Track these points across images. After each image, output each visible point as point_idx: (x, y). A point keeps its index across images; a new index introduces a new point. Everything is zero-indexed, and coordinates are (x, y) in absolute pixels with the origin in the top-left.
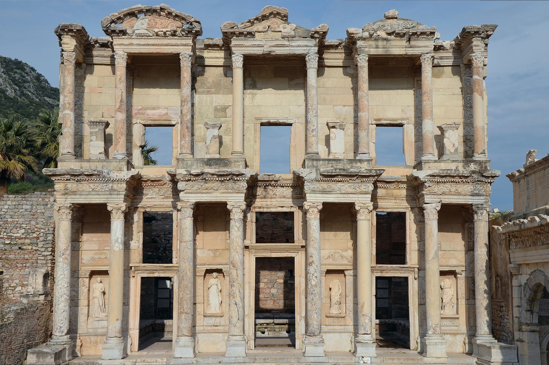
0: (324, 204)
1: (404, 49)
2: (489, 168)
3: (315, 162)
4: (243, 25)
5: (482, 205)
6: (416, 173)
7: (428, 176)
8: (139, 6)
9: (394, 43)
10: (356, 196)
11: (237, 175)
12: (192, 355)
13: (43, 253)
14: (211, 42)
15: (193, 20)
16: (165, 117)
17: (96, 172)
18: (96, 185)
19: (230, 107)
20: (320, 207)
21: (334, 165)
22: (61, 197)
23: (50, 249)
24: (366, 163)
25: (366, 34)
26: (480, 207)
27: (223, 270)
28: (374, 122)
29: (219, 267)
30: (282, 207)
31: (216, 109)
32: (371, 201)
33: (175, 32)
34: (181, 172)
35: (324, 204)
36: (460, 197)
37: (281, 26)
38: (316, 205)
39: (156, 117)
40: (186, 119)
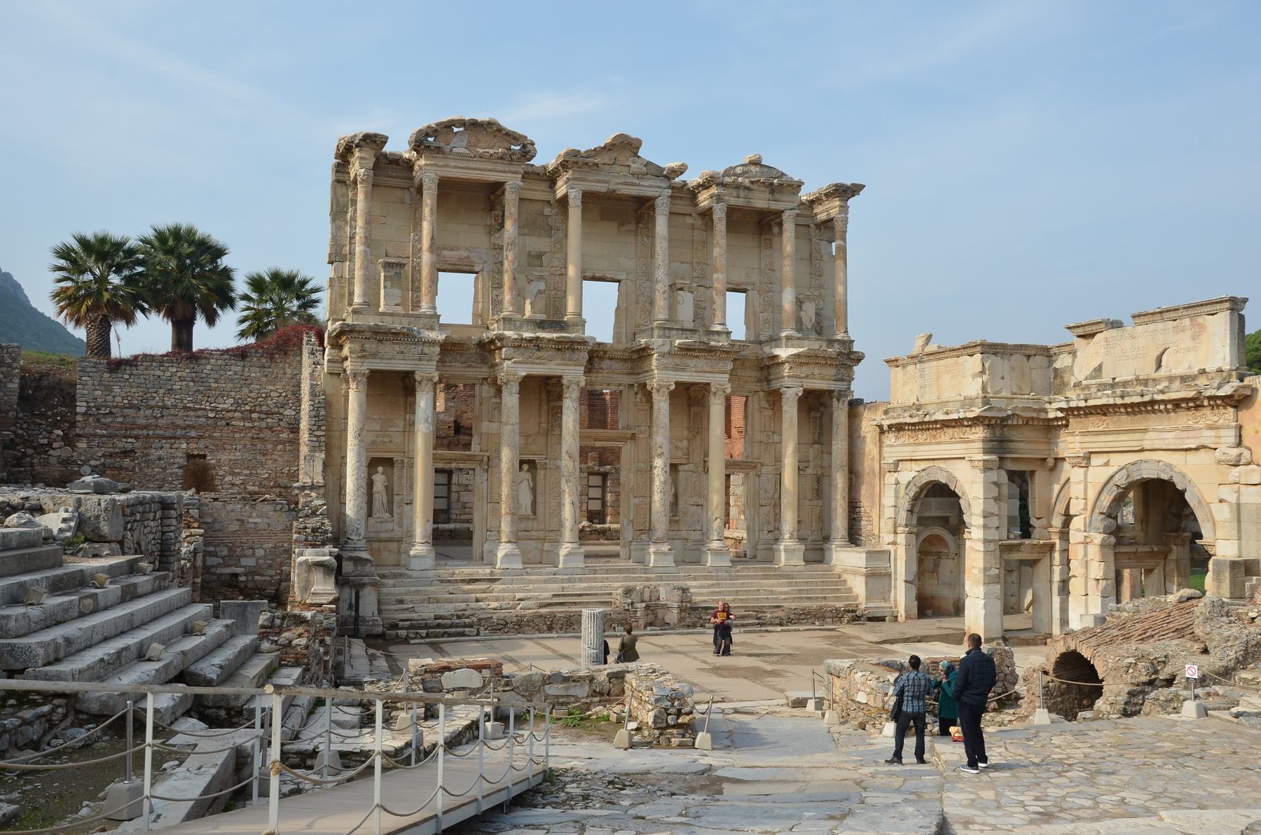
0: (677, 383)
6: (777, 352)
9: (756, 194)
11: (579, 343)
12: (521, 566)
14: (530, 170)
20: (673, 387)
25: (728, 180)
26: (841, 395)
29: (531, 457)
31: (529, 255)
32: (730, 381)
35: (677, 383)
39: (454, 261)
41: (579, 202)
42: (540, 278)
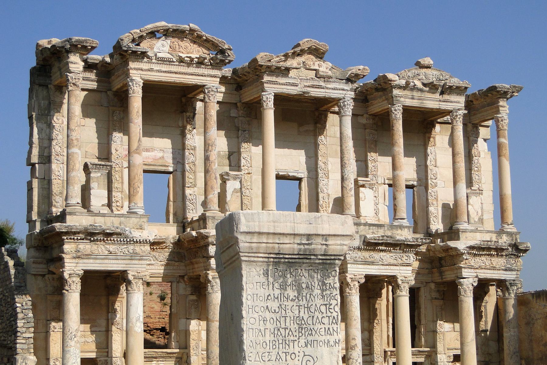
1: (438, 103)
2: (519, 241)
4: (278, 59)
5: (514, 281)
7: (467, 247)
8: (163, 23)
13: (24, 335)
15: (226, 46)
16: (161, 162)
20: (363, 281)
21: (375, 231)
22: (71, 261)
23: (32, 330)
24: (406, 230)
25: (403, 82)
28: (387, 182)
33: (205, 58)
37: (317, 63)
38: (358, 277)
39: (150, 161)
40: (214, 168)
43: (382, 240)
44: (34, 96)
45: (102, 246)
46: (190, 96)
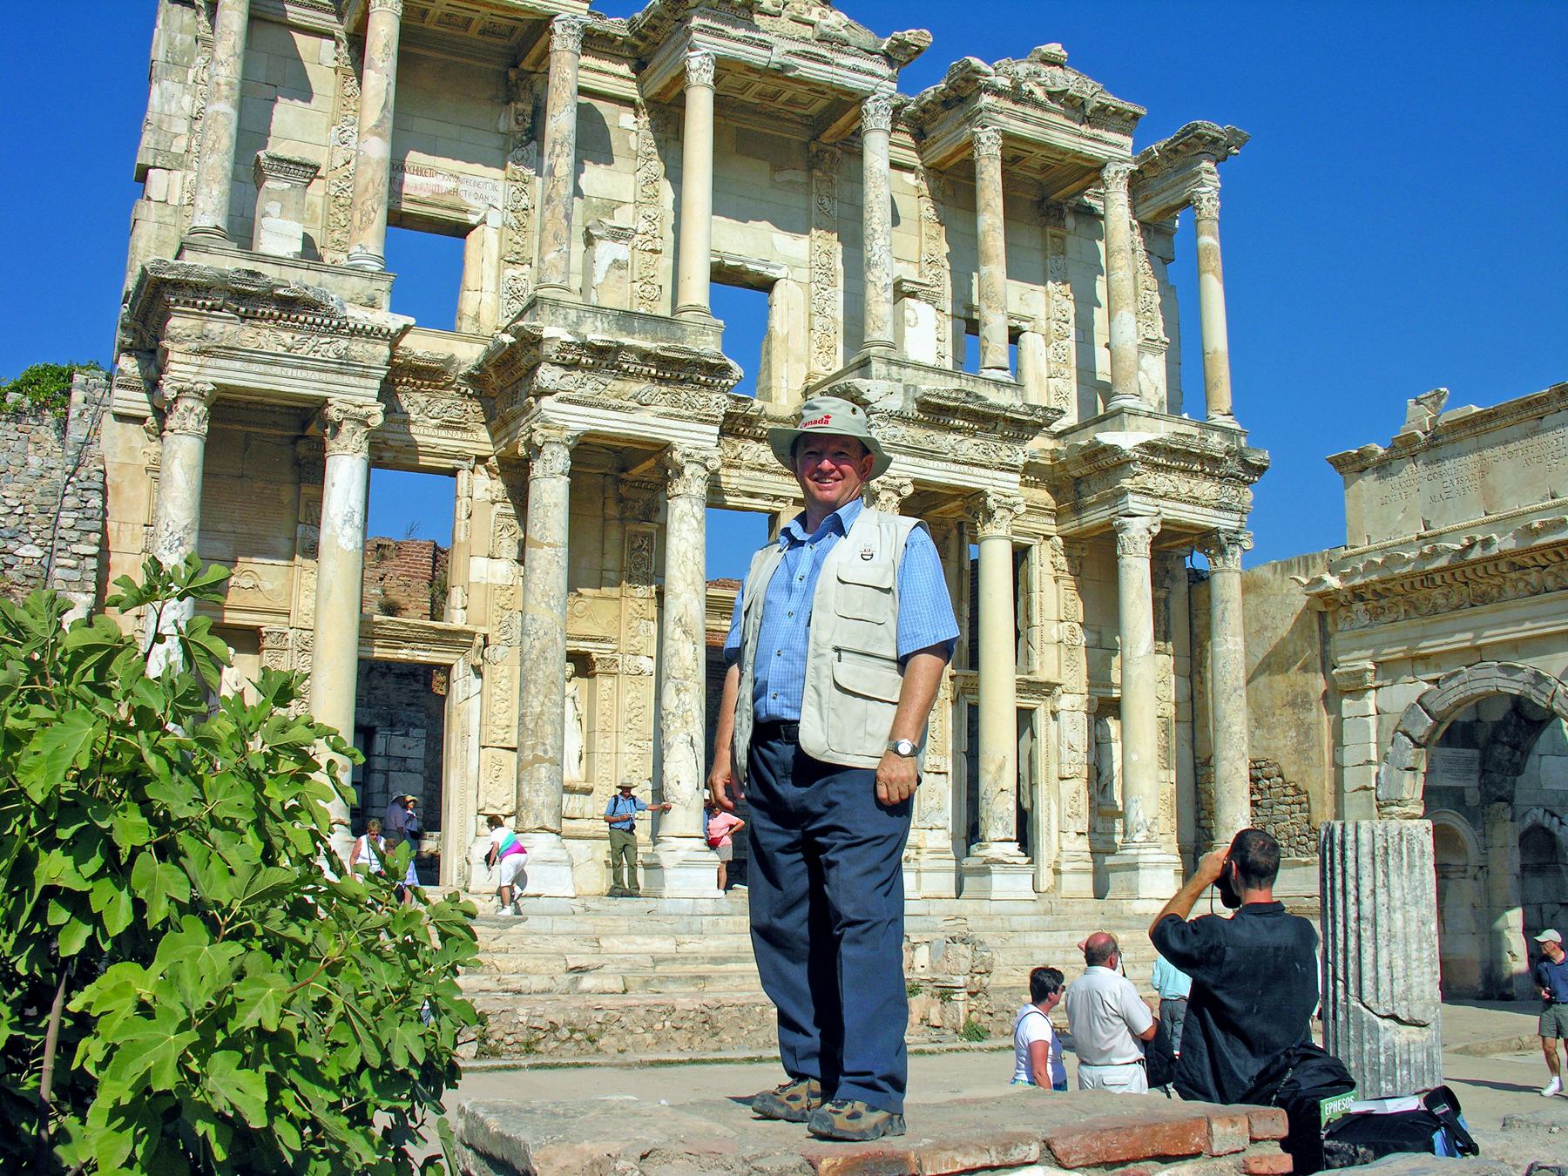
3: (894, 368)
6: (1107, 438)
7: (1141, 445)
10: (988, 473)
13: (75, 548)
16: (449, 200)
17: (310, 294)
18: (298, 337)
19: (624, 207)
20: (908, 491)
22: (184, 358)
23: (96, 537)
25: (1003, 82)
27: (594, 656)
29: (583, 646)
30: (752, 495)
34: (554, 331)
36: (1198, 509)
38: (897, 482)
39: (423, 195)
41: (708, 78)
42: (619, 234)
43: (956, 400)
44: (160, 23)
45: (267, 332)
46: (526, 65)
